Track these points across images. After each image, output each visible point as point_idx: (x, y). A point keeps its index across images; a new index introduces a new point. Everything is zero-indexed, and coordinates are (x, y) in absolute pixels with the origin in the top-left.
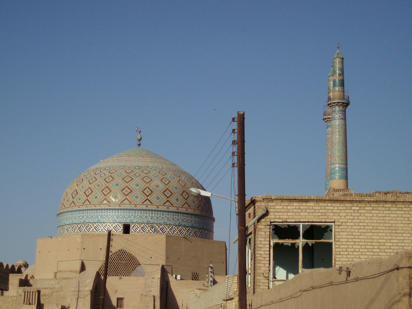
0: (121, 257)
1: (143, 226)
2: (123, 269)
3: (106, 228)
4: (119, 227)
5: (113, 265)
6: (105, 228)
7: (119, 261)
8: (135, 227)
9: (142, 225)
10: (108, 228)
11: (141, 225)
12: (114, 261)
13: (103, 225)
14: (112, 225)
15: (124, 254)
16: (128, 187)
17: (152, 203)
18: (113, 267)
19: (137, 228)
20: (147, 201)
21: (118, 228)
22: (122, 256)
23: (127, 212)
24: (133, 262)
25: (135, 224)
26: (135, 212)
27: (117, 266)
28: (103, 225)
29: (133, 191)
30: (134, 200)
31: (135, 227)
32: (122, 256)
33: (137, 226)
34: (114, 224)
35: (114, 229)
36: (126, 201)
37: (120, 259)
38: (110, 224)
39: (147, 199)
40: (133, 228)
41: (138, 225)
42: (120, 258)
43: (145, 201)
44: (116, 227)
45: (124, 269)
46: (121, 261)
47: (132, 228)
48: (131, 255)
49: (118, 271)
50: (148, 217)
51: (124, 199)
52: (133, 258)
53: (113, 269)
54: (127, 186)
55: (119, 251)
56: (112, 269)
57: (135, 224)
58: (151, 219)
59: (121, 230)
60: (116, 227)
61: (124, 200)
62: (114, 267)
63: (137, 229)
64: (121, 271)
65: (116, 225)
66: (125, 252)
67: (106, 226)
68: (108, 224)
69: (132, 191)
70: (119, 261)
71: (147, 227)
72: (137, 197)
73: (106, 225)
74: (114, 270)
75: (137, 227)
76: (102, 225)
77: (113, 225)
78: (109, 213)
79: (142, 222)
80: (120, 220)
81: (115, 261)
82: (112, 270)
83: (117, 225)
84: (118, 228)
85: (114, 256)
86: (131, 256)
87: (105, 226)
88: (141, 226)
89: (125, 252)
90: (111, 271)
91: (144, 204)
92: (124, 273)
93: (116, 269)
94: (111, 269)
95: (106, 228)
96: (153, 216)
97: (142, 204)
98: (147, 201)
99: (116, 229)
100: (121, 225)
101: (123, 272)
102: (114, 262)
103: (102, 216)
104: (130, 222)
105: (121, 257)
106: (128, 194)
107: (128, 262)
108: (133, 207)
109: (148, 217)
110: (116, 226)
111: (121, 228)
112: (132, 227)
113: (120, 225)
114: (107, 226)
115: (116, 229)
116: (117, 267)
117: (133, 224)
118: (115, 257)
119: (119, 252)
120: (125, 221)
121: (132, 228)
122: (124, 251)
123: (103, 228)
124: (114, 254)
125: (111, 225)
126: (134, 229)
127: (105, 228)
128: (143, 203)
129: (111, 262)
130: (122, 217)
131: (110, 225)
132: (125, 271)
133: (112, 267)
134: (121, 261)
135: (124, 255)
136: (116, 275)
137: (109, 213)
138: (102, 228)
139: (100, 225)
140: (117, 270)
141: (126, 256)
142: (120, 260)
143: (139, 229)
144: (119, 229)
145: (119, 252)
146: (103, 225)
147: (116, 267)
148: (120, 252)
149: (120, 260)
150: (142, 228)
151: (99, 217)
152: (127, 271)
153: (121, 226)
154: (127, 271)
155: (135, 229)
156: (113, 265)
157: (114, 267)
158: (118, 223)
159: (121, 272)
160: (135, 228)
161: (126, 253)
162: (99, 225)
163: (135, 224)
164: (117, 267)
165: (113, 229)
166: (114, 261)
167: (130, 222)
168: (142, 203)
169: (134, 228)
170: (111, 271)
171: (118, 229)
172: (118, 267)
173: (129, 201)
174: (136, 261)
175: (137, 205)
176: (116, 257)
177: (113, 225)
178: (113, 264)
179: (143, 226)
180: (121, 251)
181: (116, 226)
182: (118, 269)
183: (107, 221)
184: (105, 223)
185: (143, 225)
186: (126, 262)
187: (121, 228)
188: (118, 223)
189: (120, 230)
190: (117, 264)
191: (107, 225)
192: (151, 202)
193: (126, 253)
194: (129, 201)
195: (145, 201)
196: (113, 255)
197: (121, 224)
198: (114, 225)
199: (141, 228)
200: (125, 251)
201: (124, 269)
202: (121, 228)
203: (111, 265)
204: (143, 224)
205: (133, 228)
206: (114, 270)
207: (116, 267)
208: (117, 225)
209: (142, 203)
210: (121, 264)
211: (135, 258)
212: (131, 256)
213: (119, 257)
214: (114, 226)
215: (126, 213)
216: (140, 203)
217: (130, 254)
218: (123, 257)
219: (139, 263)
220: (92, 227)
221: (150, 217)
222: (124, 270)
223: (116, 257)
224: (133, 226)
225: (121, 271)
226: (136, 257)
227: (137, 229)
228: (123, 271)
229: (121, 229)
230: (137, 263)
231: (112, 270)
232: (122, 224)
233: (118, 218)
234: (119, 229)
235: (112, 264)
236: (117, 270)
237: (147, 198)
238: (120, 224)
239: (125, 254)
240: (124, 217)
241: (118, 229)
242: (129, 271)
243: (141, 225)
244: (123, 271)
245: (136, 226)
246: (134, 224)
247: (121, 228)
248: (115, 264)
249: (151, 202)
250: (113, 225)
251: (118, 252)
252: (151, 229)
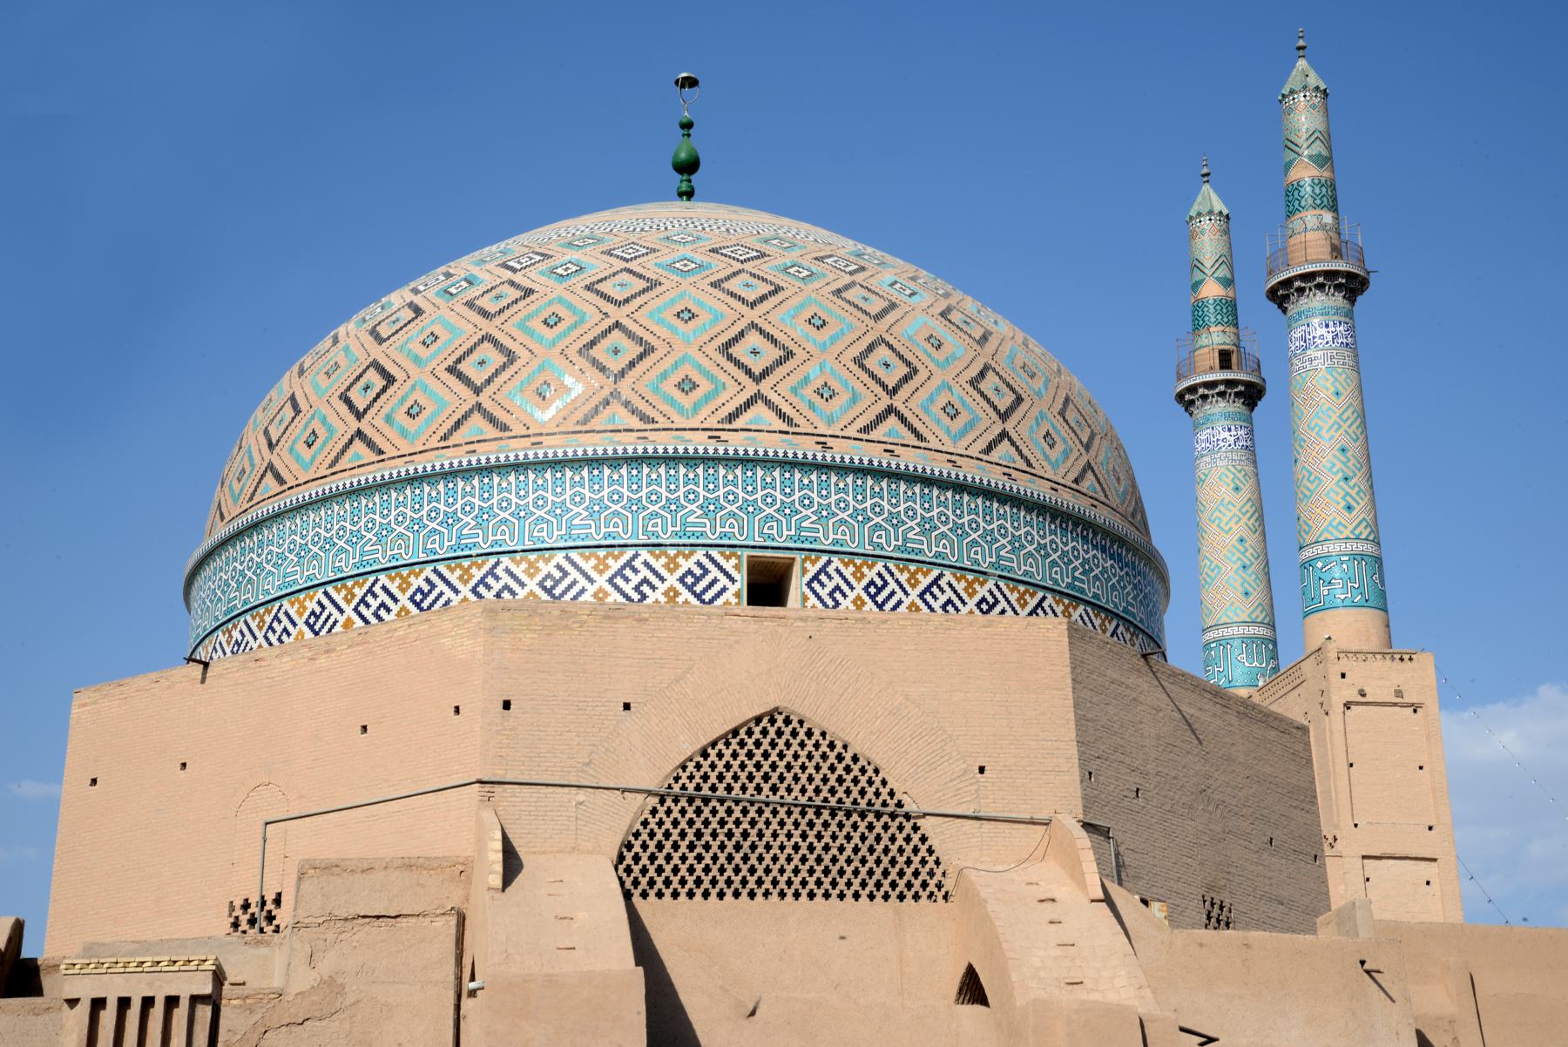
0: (774, 766)
1: (880, 575)
2: (789, 850)
3: (633, 584)
4: (721, 576)
5: (722, 823)
6: (619, 581)
7: (759, 789)
8: (830, 577)
9: (870, 567)
10: (641, 584)
11: (865, 569)
12: (721, 792)
13: (610, 561)
14: (672, 566)
15: (795, 747)
16: (761, 331)
17: (919, 436)
18: (721, 837)
19: (837, 588)
20: (892, 419)
21: (715, 581)
22: (781, 756)
23: (769, 480)
24: (855, 802)
25: (825, 558)
26: (824, 485)
27: (745, 825)
28: (607, 567)
29: (800, 355)
30: (812, 406)
31: (830, 577)
32: (781, 756)
33: (838, 571)
34: (687, 557)
35: (690, 588)
36: (760, 409)
37: (766, 778)
38: (657, 557)
39: (890, 410)
40: (816, 585)
41: (846, 565)
42: (766, 768)
43: (881, 418)
44: (698, 579)
45: (796, 848)
46: (774, 789)
47: (809, 584)
48: (839, 749)
49: (742, 866)
50: (904, 523)
51: (742, 399)
52: (856, 768)
53: (722, 847)
54: (753, 325)
55: (758, 720)
56: (715, 845)
57: (829, 562)
58: (922, 533)
59: (738, 595)
60: (703, 576)
61: (748, 404)
62: (730, 835)
63: (844, 595)
64: (775, 859)
65: (699, 564)
66: (794, 734)
67: (628, 572)
68: (644, 554)
69: (789, 354)
70: (759, 789)
71: (901, 586)
72: (826, 393)
73: (629, 564)
74: (730, 858)
75: (837, 580)
76: (601, 567)
77: (681, 560)
78: (649, 484)
79: (869, 550)
80: (727, 529)
81: (729, 789)
82: (715, 858)
83: (705, 562)
84: (715, 581)
85: (720, 755)
86: (840, 758)
87: (620, 573)
88: (863, 575)
89: (794, 734)
90: (708, 860)
91: (874, 435)
92: (797, 881)
93: (738, 847)
94: (707, 847)
95: (627, 580)
96: (931, 519)
97: (865, 436)
98: (892, 419)
99: (698, 589)
100: (734, 561)
101: (789, 868)
102: (722, 801)
103: (596, 508)
104: (792, 545)
105: (774, 766)
106: (765, 373)
107: (826, 800)
108: (807, 448)
109: (904, 523)
110: (698, 572)
111: (738, 585)
112: (811, 581)
113: (729, 566)
114: (635, 571)
115: (698, 589)
116: (745, 835)
117: (814, 563)
118: (728, 766)
119: (757, 730)
120: (759, 541)
121: (809, 584)
122: (787, 721)
123: (610, 581)
124: (720, 746)
125: (666, 566)
126: (824, 593)
127: (619, 581)
128: (866, 429)
129: (706, 801)
130: (740, 508)
131: (658, 565)
132: (804, 860)
133: (714, 835)
134: (774, 789)
135: (789, 754)
136: (745, 892)
137: (649, 484)
138: (601, 581)
139: (588, 566)
140: (745, 859)
141: (810, 756)
142: (766, 787)
143: (852, 595)
144: (724, 589)
145: (757, 730)
146: (607, 567)
147: (737, 837)
148: (765, 732)
149: (766, 787)
150: (872, 590)
151: (576, 510)
152: (819, 860)
153: (737, 567)
154: (819, 860)
155: (831, 594)
156: (722, 823)
157: (730, 835)
158: (714, 553)
159: (775, 873)
160: (830, 586)
161: (802, 736)
162: (574, 564)
163: (829, 562)
164: (745, 835)
165: (679, 587)
166: (721, 792)
167: (799, 545)
168: (860, 431)
169: (823, 585)
170: (708, 860)
171: (717, 588)
172: (753, 832)
173: (782, 415)
174: (877, 794)
175: (830, 442)
176: (736, 764)
177: (681, 560)
178: (722, 813)
179: (880, 575)
180: (773, 721)
181: (698, 572)
182: (753, 847)
183: (635, 534)
184: (621, 554)
185: (875, 570)
186: (810, 799)
187: (733, 580)
188: (714, 553)
189: (728, 596)
190: (745, 812)
191: (637, 563)
192: (914, 431)
193: (802, 736)
194: (782, 415)
195: (881, 418)
196: (713, 753)
197: (734, 554)
198: (686, 565)
199: (868, 586)
200: (795, 724)
201: (796, 848)
202: (733, 580)
203: (706, 823)
204: (879, 566)
205: (816, 585)
206: (730, 858)
207: (737, 837)
208: (705, 562)
209: (860, 431)
210: (775, 813)
211: (870, 773)
212: (840, 758)
213: (758, 766)
214: (690, 572)
215: (763, 488)
216: (852, 431)
217: (832, 746)
218: (789, 767)
219: (899, 804)
220: (524, 578)
221: (918, 525)
222: (796, 858)
223: (736, 764)
224: (812, 570)
225: (775, 859)
226: (878, 761)
227: (844, 595)
228: (789, 859)
229: (733, 589)
230: (884, 804)
231: (715, 858)
232: (739, 557)
233: (711, 515)
234: (724, 589)
235: (714, 812)
236: (745, 859)
237: (886, 401)
238: (728, 558)
239: (802, 745)
240: (751, 509)
241: (717, 588)
242: (834, 860)
243: (865, 569)
244: (789, 859)
245: (834, 574)
246: (818, 559)
247: (738, 585)
248: (729, 812)
249: (914, 431)
250: (677, 566)
251: (750, 733)
252: (925, 601)
